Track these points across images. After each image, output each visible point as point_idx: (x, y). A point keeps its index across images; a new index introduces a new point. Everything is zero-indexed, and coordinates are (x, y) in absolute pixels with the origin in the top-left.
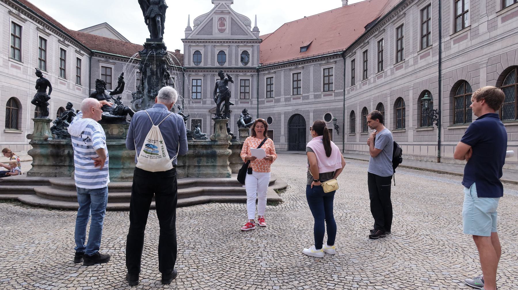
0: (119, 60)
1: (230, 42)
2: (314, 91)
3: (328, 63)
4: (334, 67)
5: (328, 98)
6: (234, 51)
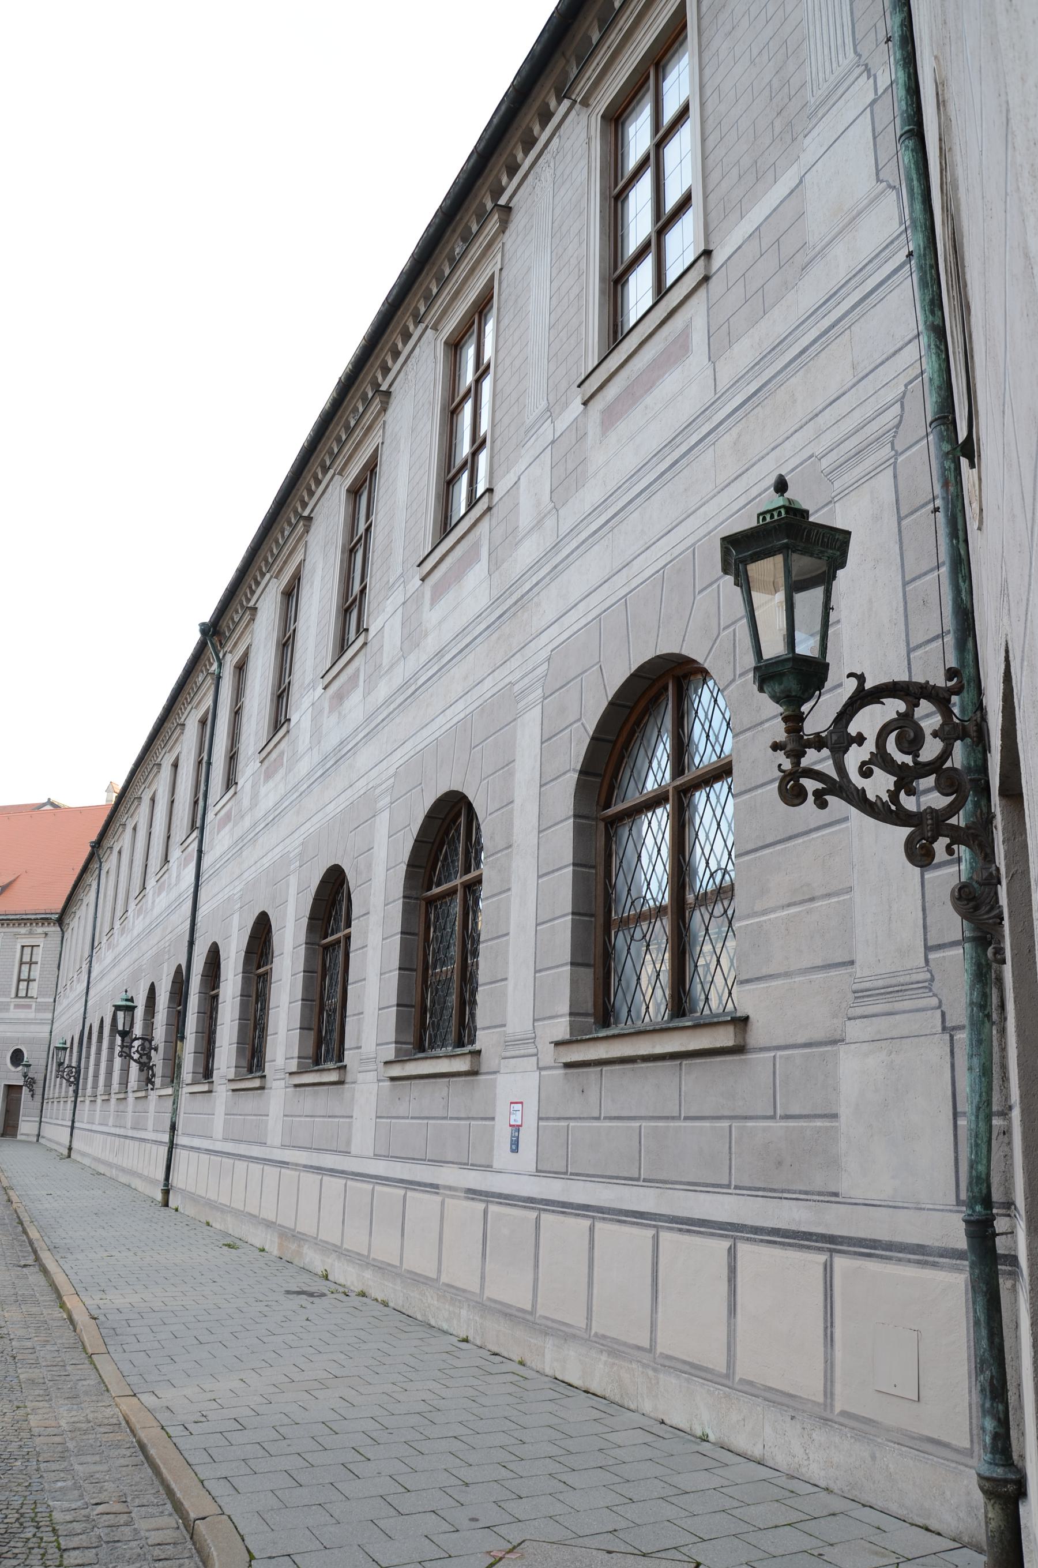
4: (42, 945)
5: (22, 1014)
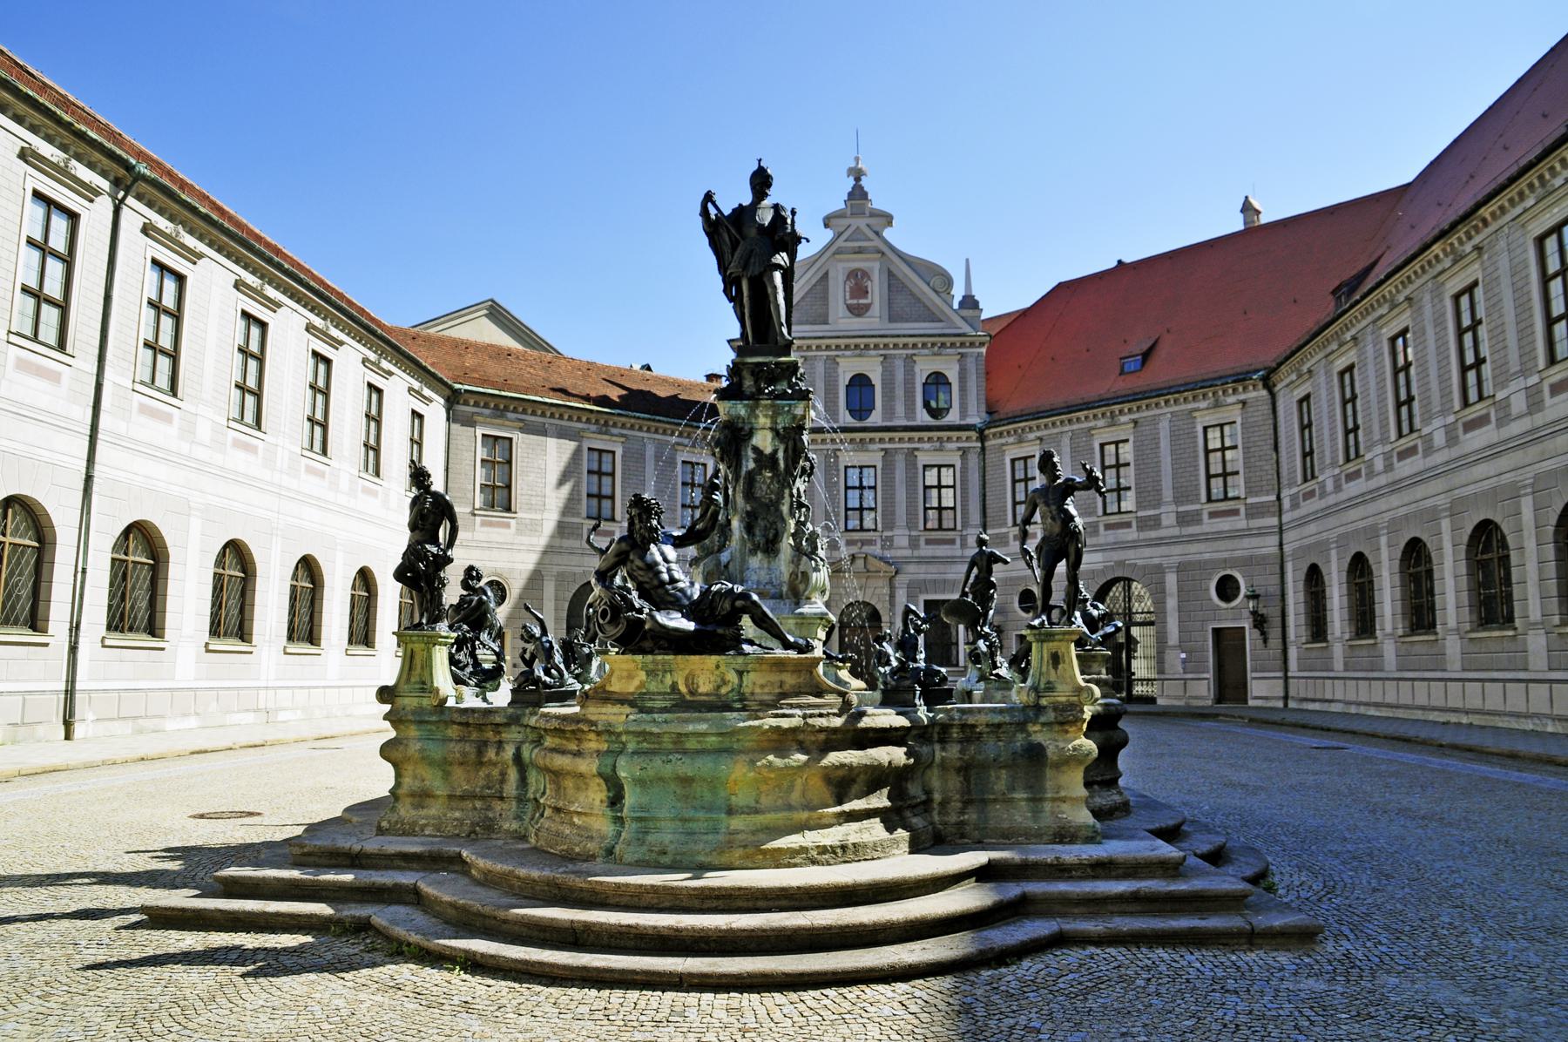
0: (534, 413)
1: (886, 346)
2: (1177, 501)
3: (1217, 405)
5: (1225, 524)
6: (900, 376)
